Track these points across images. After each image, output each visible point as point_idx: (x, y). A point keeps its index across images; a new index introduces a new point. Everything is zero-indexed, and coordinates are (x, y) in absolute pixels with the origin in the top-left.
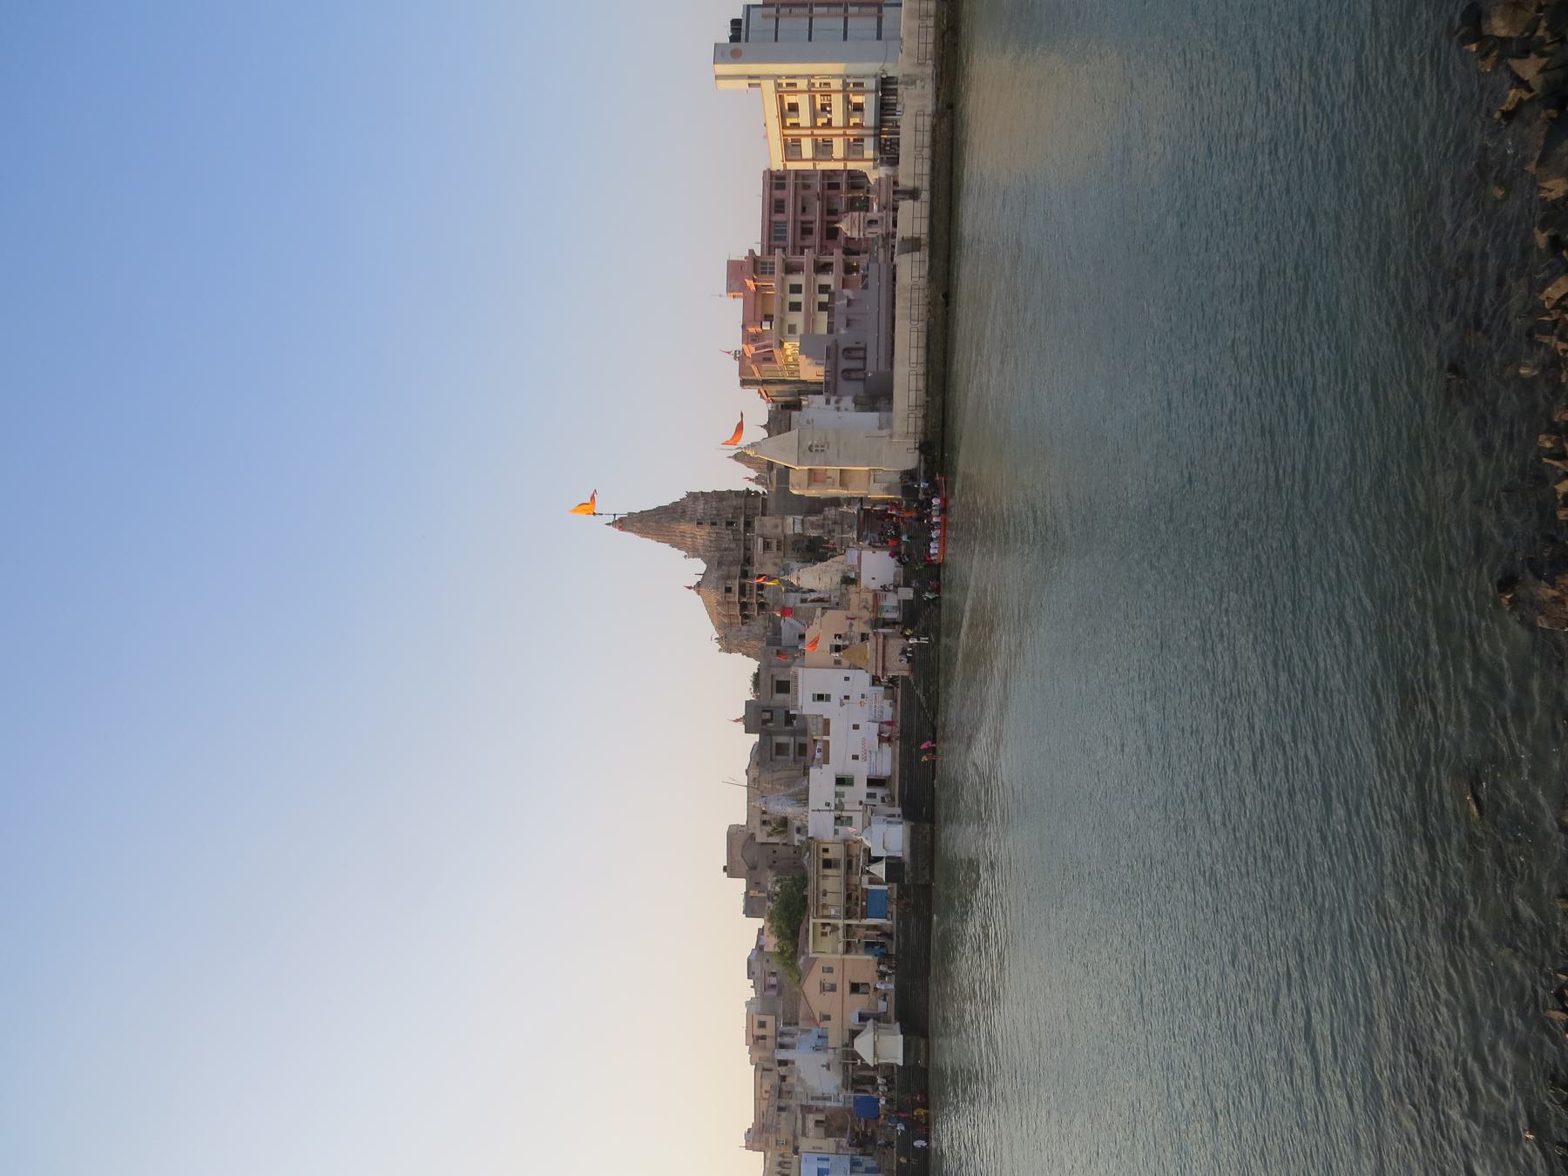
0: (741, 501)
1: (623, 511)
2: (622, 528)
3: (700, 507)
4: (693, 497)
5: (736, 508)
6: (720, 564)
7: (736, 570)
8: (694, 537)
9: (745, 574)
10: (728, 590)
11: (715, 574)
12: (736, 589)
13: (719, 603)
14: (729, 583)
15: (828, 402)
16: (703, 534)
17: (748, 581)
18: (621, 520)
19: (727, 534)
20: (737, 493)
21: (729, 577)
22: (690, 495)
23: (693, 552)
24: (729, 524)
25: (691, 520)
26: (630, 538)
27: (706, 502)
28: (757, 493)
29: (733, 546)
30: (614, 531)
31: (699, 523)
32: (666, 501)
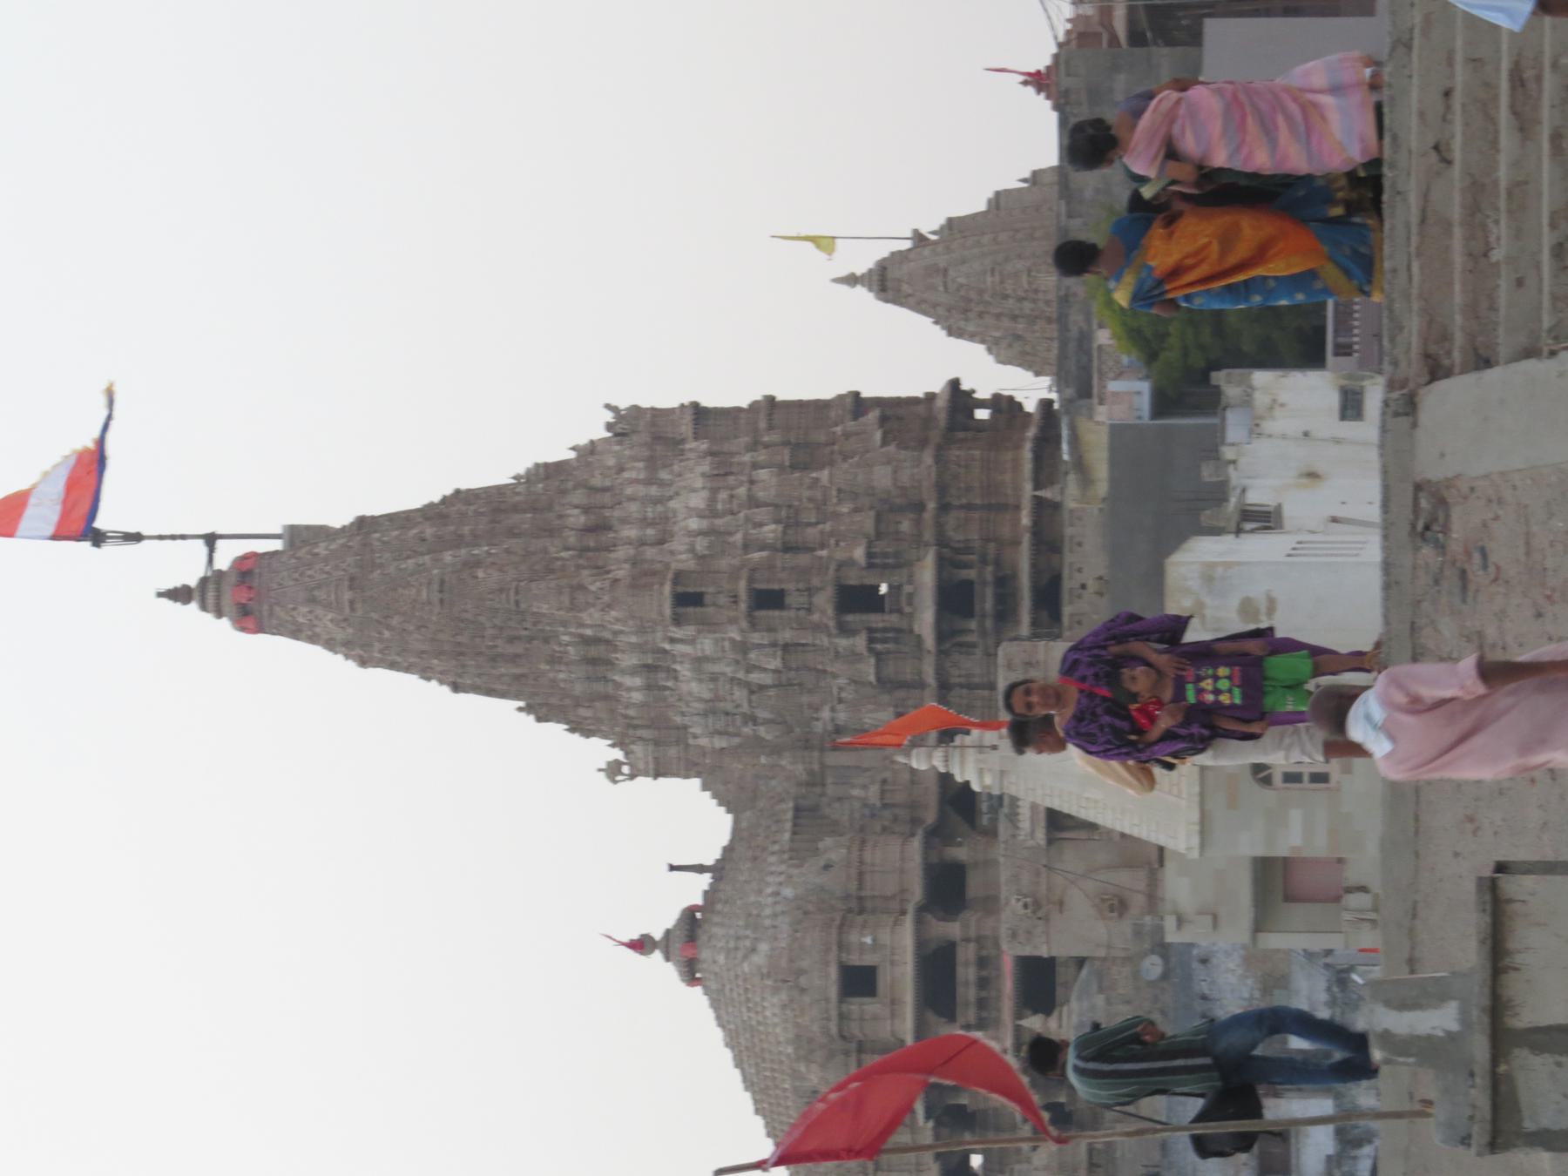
0: (919, 469)
1: (259, 514)
2: (250, 618)
3: (690, 499)
4: (646, 433)
5: (887, 509)
6: (808, 817)
7: (902, 863)
8: (655, 668)
9: (947, 889)
10: (859, 981)
11: (780, 885)
12: (901, 976)
13: (805, 1045)
14: (864, 944)
15: (1351, 406)
16: (703, 660)
17: (953, 929)
18: (246, 568)
19: (847, 659)
20: (896, 417)
21: (859, 906)
22: (631, 425)
23: (654, 746)
24: (856, 599)
25: (644, 576)
26: (298, 672)
27: (722, 470)
28: (1005, 406)
29: (879, 716)
30: (215, 632)
31: (687, 600)
32: (495, 466)
